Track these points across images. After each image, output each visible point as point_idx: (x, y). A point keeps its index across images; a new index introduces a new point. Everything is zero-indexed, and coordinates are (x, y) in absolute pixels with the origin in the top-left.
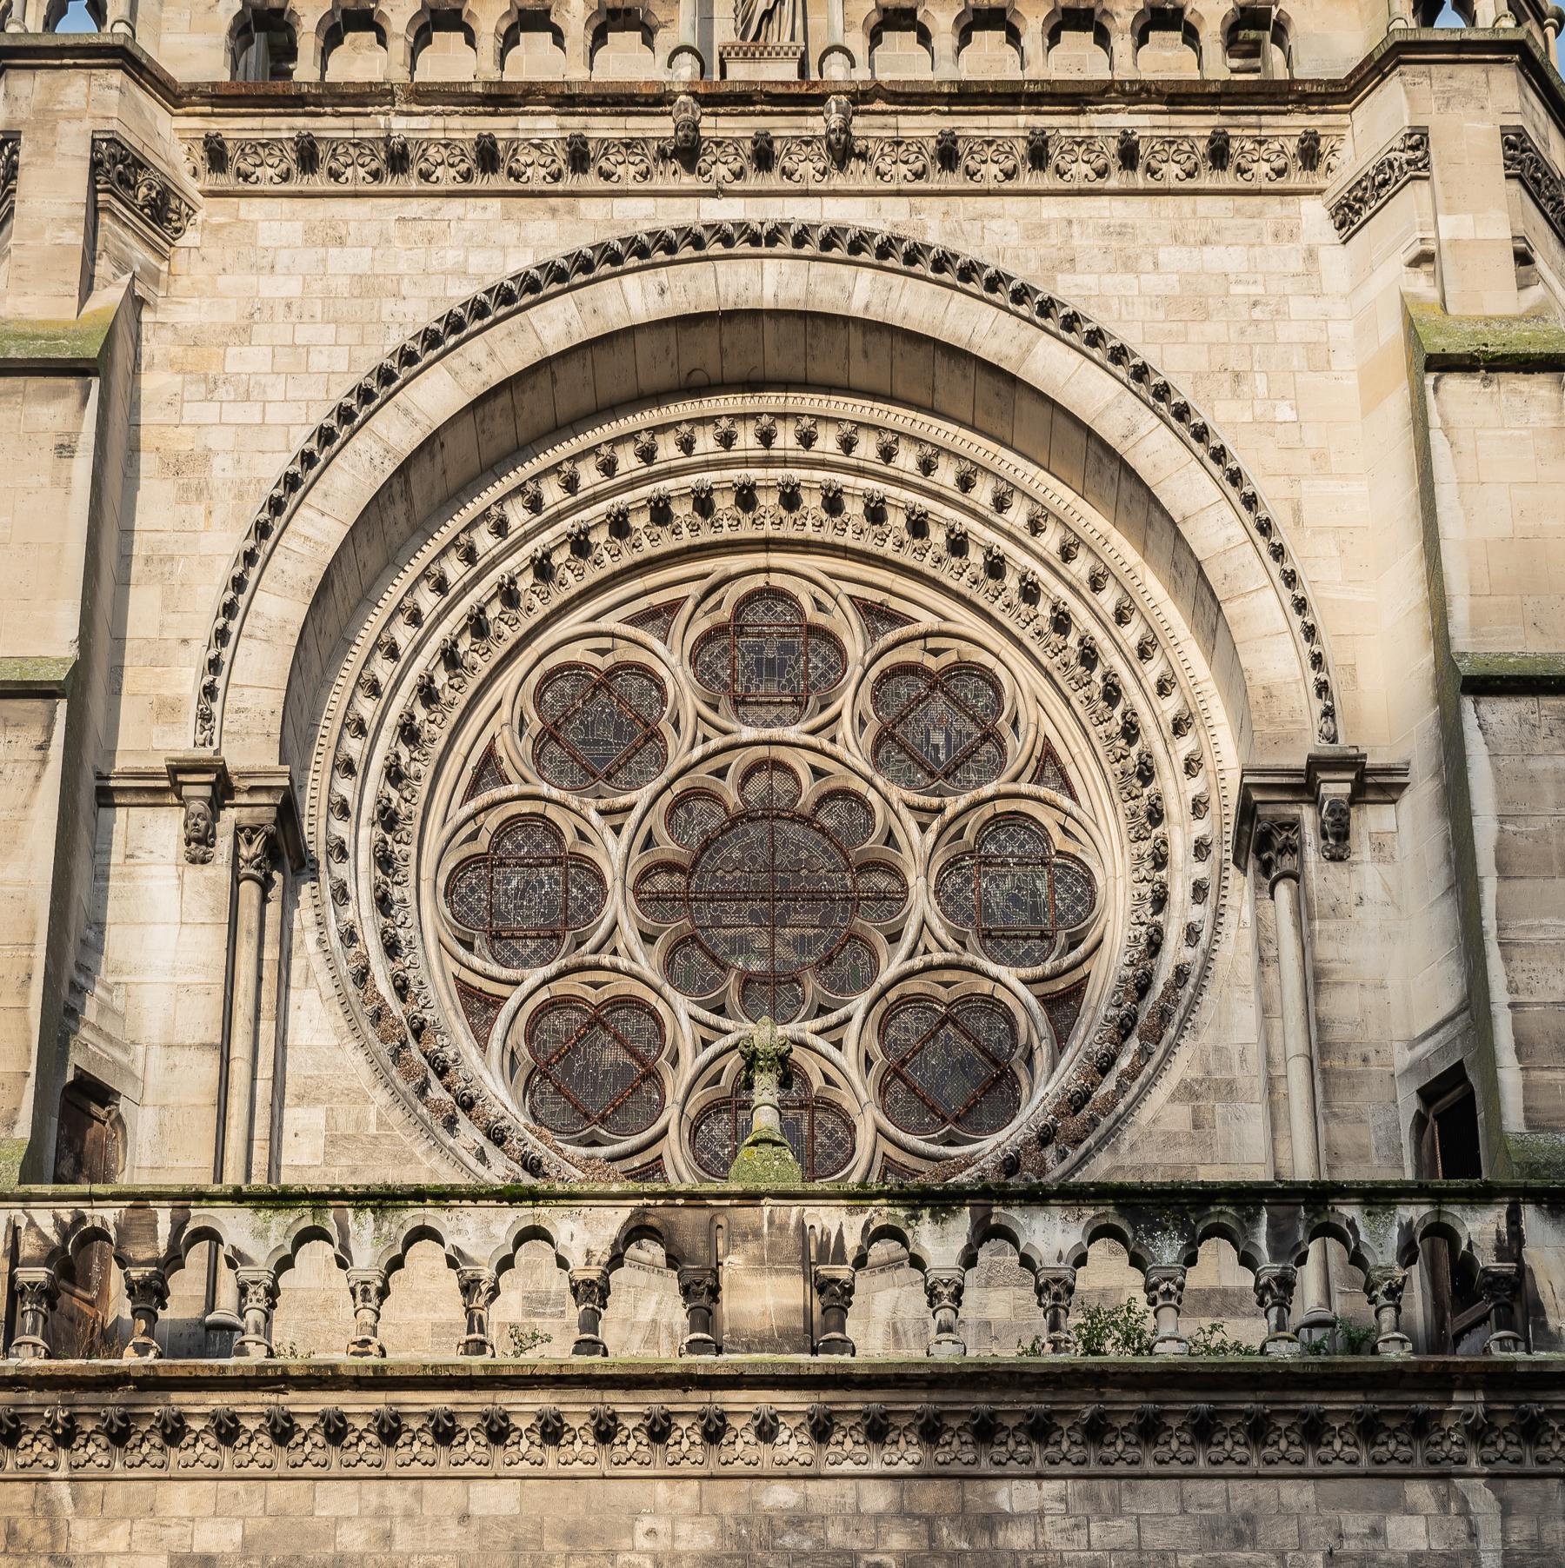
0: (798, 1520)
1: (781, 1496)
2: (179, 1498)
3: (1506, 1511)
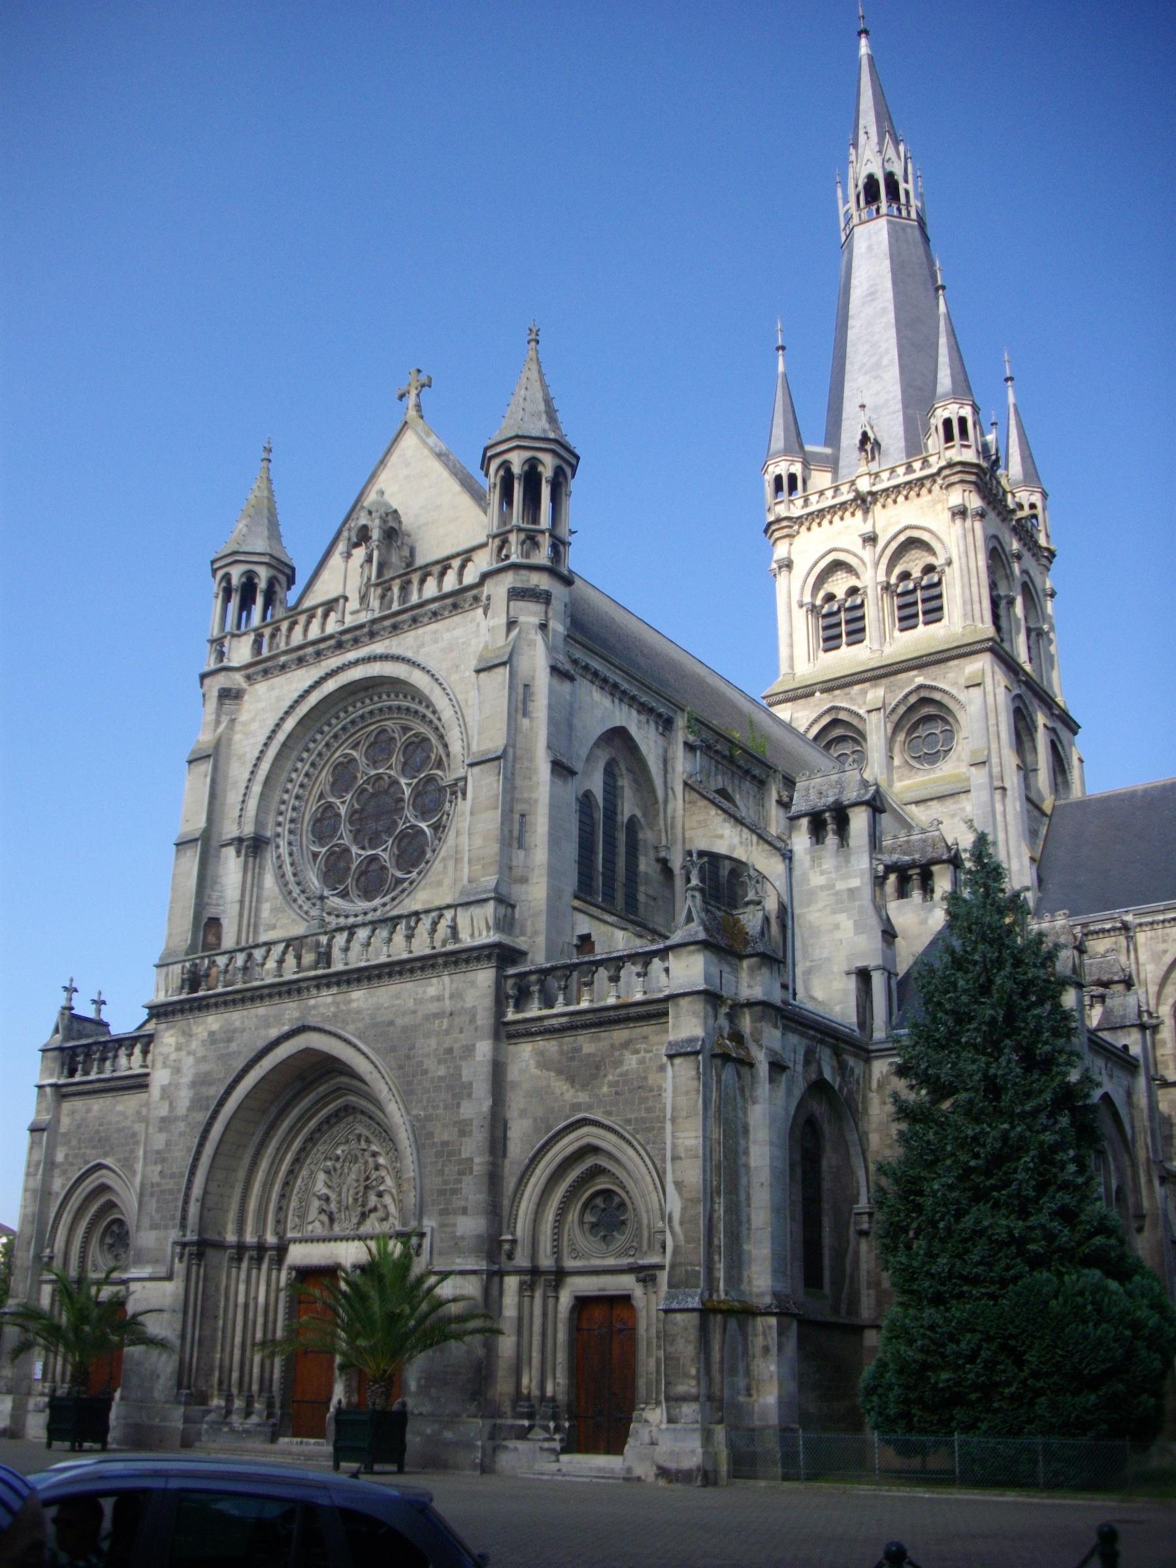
0: (315, 1007)
1: (312, 1002)
2: (210, 1019)
3: (452, 981)
